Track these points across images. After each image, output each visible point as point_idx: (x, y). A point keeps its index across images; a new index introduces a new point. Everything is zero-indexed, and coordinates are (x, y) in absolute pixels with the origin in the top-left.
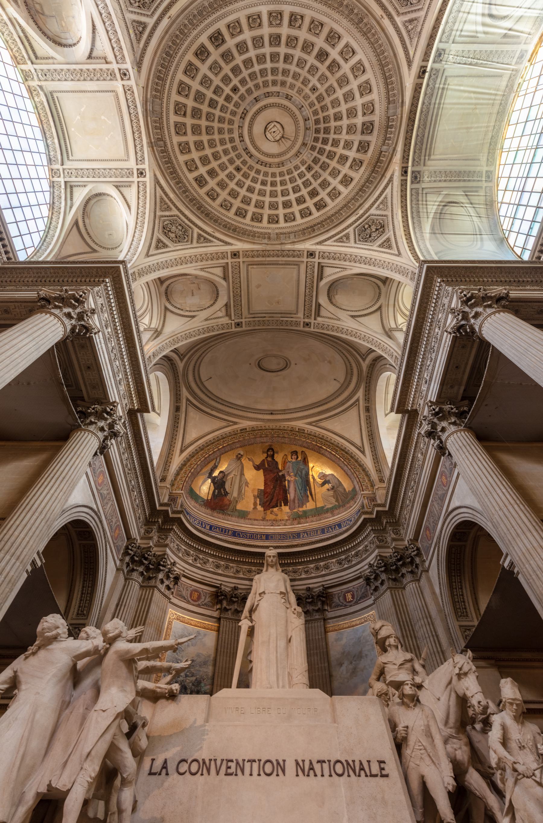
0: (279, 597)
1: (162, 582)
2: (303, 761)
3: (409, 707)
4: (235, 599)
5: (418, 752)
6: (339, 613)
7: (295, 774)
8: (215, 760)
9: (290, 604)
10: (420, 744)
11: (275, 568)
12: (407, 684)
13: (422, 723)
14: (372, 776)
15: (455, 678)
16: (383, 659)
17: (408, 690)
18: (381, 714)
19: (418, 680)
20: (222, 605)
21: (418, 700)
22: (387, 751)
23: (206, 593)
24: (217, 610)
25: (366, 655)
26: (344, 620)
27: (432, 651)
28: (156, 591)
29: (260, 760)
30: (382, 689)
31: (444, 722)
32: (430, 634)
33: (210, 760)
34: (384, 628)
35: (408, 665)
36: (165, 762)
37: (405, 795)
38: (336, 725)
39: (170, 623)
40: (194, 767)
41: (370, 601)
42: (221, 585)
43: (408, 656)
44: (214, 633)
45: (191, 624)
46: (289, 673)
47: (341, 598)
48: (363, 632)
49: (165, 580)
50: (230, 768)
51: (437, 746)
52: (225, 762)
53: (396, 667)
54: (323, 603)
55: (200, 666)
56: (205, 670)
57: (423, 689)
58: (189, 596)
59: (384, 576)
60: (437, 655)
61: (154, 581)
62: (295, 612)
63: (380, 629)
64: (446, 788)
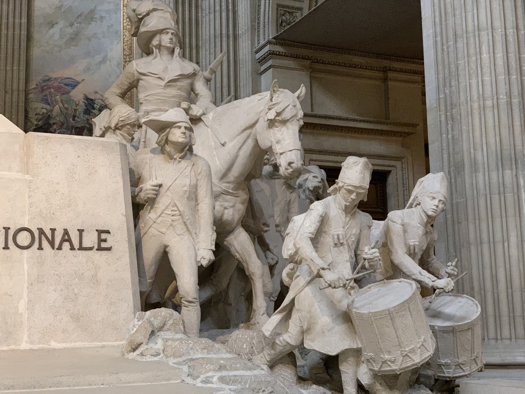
3: (171, 158)
5: (169, 219)
12: (180, 127)
13: (187, 181)
14: (81, 248)
15: (262, 125)
16: (140, 65)
17: (177, 135)
18: (119, 166)
19: (196, 110)
21: (191, 150)
27: (218, 32)
31: (220, 175)
32: (224, 8)
34: (155, 13)
35: (185, 83)
37: (131, 272)
38: (28, 177)
43: (189, 67)
51: (200, 211)
53: (163, 83)
57: (201, 124)
63: (148, 14)
64: (197, 262)
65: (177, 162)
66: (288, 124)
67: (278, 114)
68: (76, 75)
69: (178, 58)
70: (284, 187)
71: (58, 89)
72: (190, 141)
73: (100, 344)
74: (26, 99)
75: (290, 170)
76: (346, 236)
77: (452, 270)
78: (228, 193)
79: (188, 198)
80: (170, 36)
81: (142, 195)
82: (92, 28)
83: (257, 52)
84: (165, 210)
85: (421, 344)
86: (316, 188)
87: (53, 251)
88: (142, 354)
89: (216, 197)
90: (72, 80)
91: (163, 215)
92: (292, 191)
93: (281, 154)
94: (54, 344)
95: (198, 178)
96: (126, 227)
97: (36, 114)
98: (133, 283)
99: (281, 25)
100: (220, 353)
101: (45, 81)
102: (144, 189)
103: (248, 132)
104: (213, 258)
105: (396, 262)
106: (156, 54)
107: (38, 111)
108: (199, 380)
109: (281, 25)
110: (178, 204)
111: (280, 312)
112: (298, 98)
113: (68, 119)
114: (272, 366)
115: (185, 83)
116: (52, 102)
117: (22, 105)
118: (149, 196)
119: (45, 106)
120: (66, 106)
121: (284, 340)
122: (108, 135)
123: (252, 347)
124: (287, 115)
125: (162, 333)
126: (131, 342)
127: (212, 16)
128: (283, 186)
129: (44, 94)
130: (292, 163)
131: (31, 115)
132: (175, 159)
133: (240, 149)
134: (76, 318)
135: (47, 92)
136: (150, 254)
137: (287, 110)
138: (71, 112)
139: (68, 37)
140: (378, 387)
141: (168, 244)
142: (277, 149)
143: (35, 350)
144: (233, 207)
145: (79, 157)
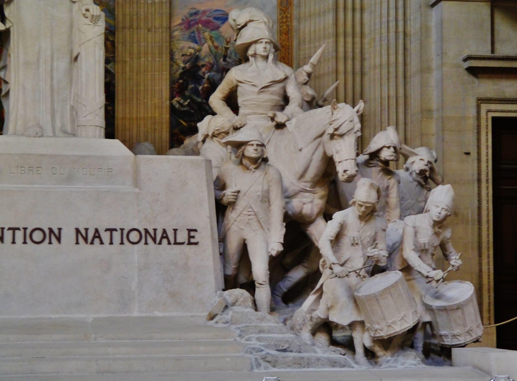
2: (87, 230)
3: (248, 169)
7: (75, 241)
10: (251, 210)
12: (252, 145)
13: (260, 188)
14: (176, 243)
17: (250, 152)
18: (204, 179)
19: (281, 117)
21: (265, 160)
22: (204, 217)
29: (25, 229)
30: (223, 128)
31: (298, 176)
34: (251, 23)
35: (277, 88)
37: (214, 261)
38: (137, 190)
43: (281, 71)
46: (72, 108)
53: (256, 90)
65: (252, 172)
66: (346, 138)
67: (336, 130)
68: (226, 6)
69: (272, 64)
70: (381, 173)
71: (207, 24)
72: (263, 155)
73: (190, 314)
74: (171, 37)
76: (360, 237)
77: (455, 262)
79: (261, 201)
84: (243, 211)
85: (401, 318)
86: (422, 173)
87: (155, 246)
88: (217, 322)
89: (288, 197)
90: (221, 13)
91: (241, 215)
92: (389, 177)
93: (340, 162)
94: (158, 314)
95: (270, 184)
96: (209, 227)
97: (183, 55)
98: (215, 270)
101: (191, 15)
102: (226, 195)
103: (319, 140)
105: (405, 256)
106: (252, 62)
108: (244, 339)
110: (253, 206)
113: (218, 59)
114: (314, 333)
115: (277, 88)
116: (200, 40)
117: (166, 45)
118: (230, 200)
119: (193, 45)
120: (216, 44)
121: (317, 315)
122: (208, 140)
123: (304, 320)
125: (234, 308)
126: (210, 314)
128: (379, 174)
129: (191, 30)
130: (347, 171)
131: (177, 56)
132: (251, 170)
133: (313, 154)
134: (173, 295)
135: (194, 29)
136: (233, 245)
137: (344, 125)
138: (221, 51)
140: (378, 350)
141: (246, 238)
142: (336, 159)
143: (143, 317)
144: (311, 202)
145: (174, 173)
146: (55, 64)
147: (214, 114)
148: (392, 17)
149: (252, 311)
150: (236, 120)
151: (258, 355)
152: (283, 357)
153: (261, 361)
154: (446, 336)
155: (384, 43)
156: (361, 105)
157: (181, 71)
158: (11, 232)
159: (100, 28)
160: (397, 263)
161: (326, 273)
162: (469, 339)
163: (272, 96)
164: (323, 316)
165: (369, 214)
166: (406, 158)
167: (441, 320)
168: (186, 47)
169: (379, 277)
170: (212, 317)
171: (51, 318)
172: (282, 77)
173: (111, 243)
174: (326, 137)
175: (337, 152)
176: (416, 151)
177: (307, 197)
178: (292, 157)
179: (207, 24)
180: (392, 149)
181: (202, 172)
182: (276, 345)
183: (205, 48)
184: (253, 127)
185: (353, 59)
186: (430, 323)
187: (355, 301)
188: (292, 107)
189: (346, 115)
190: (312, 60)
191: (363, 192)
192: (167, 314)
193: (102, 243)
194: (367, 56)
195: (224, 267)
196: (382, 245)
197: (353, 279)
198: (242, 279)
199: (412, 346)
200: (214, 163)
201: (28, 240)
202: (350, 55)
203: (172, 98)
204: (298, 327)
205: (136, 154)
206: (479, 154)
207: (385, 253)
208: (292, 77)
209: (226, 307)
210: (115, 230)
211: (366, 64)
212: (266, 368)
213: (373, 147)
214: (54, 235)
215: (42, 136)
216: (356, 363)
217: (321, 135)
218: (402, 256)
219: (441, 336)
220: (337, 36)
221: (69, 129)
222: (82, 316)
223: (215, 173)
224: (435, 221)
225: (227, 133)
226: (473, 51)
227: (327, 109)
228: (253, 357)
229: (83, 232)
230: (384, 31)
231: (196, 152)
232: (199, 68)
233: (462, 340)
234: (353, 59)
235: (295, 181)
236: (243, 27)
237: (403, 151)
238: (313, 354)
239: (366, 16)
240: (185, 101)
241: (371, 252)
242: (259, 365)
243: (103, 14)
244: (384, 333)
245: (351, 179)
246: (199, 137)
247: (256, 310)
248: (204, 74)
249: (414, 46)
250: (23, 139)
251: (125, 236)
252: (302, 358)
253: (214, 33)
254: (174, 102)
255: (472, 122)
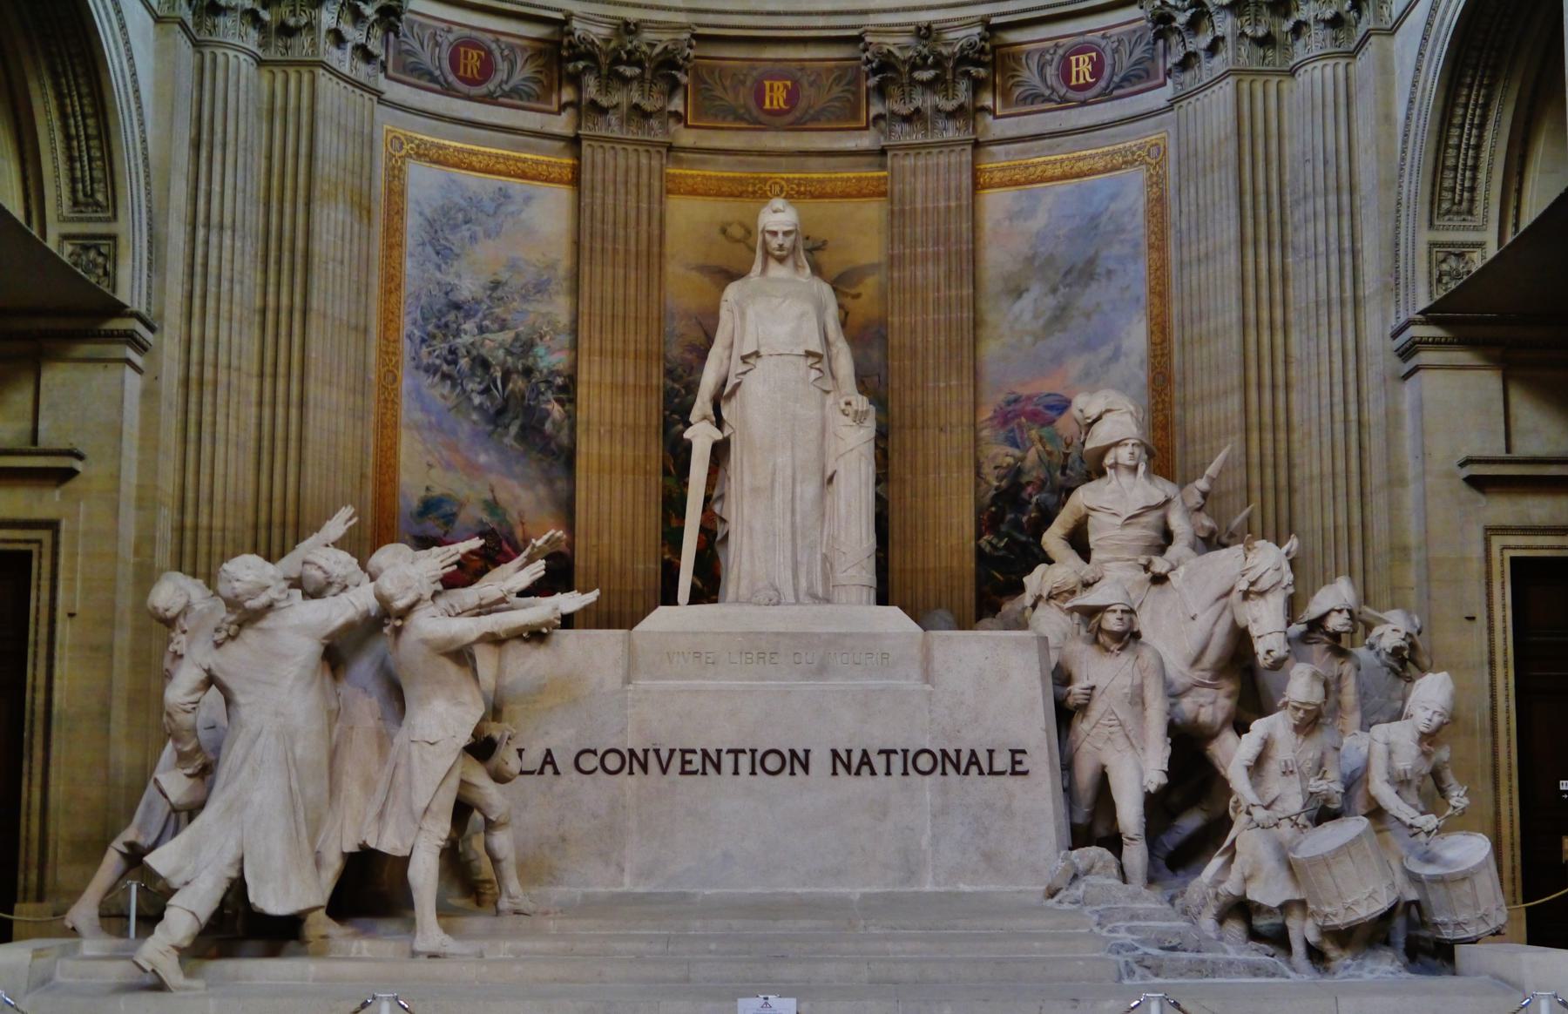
0: (804, 363)
1: (338, 38)
2: (849, 752)
3: (1107, 650)
4: (629, 71)
6: (1032, 124)
8: (657, 752)
9: (834, 377)
11: (790, 262)
13: (1128, 681)
14: (991, 773)
17: (1112, 622)
18: (1037, 667)
19: (1160, 565)
20: (579, 89)
21: (1136, 636)
23: (512, 48)
24: (563, 107)
25: (1110, 273)
26: (1051, 150)
27: (1323, 296)
28: (324, 80)
29: (753, 751)
31: (1191, 659)
32: (1334, 247)
33: (646, 751)
36: (549, 752)
38: (928, 687)
39: (395, 174)
40: (613, 762)
41: (1157, 98)
42: (569, 16)
43: (1159, 490)
44: (564, 193)
45: (471, 168)
46: (825, 558)
47: (1051, 72)
48: (1113, 197)
49: (348, 30)
50: (690, 762)
52: (677, 755)
53: (1119, 521)
54: (977, 86)
55: (524, 298)
56: (544, 309)
58: (446, 64)
59: (1225, 25)
60: (1336, 309)
61: (305, 40)
62: (849, 410)
63: (1099, 418)
66: (1269, 597)
67: (1253, 584)
71: (1034, 416)
73: (1015, 888)
74: (977, 440)
75: (1270, 661)
78: (1204, 685)
80: (1128, 449)
81: (1071, 700)
82: (1094, 295)
83: (1395, 336)
86: (1396, 652)
87: (959, 777)
88: (1060, 902)
89: (1174, 695)
94: (964, 887)
99: (1439, 281)
100: (1151, 901)
101: (1008, 403)
103: (1223, 601)
104: (1164, 780)
105: (1373, 793)
107: (999, 461)
109: (1439, 281)
111: (1222, 854)
112: (1287, 554)
114: (1221, 920)
116: (1023, 443)
119: (1011, 450)
122: (1040, 604)
124: (1263, 584)
125: (1088, 878)
126: (1048, 888)
127: (1311, 263)
131: (987, 469)
133: (1215, 624)
134: (988, 857)
135: (1014, 425)
136: (1085, 775)
139: (1048, 314)
142: (1254, 631)
144: (1213, 703)
146: (798, 489)
147: (1050, 562)
148: (1338, 398)
149: (1119, 883)
150: (1087, 571)
151: (1129, 957)
152: (1172, 960)
153: (1135, 967)
154: (1445, 925)
155: (1327, 440)
156: (1293, 544)
157: (993, 492)
158: (732, 756)
159: (868, 431)
160: (1360, 804)
161: (1240, 820)
162: (1483, 929)
163: (1145, 531)
164: (1235, 892)
165: (1310, 723)
166: (1369, 627)
167: (1435, 897)
168: (1000, 454)
169: (1329, 828)
170: (1052, 894)
171: (794, 894)
172: (1161, 499)
173: (888, 773)
174: (1236, 597)
175: (1255, 621)
176: (1385, 616)
177: (1206, 695)
178: (1180, 628)
179: (1034, 416)
180: (1345, 614)
181: (1033, 657)
182: (1159, 941)
183: (1032, 456)
184: (1115, 583)
185: (1275, 466)
186: (1417, 903)
187: (1291, 867)
188: (1178, 549)
189: (1267, 559)
190: (1208, 472)
191: (1300, 686)
192: (979, 889)
193: (873, 773)
194: (1297, 461)
195: (1071, 811)
196: (1333, 774)
197: (1286, 830)
198: (1101, 830)
199: (1387, 942)
200: (1052, 641)
201: (758, 769)
202: (1269, 459)
203: (979, 536)
204: (1194, 910)
205: (925, 630)
206: (1490, 618)
207: (1338, 787)
208: (1178, 499)
209: (1075, 877)
210: (895, 752)
211: (1297, 473)
212: (1143, 977)
213: (1314, 610)
214: (798, 761)
215: (778, 603)
216: (1294, 970)
217: (1228, 594)
218: (1368, 791)
219: (1436, 924)
220: (1247, 430)
221: (820, 591)
222: (842, 890)
223: (1054, 658)
224: (1422, 733)
225: (1073, 592)
226: (1476, 448)
227: (1237, 549)
228: (1121, 959)
229: (844, 756)
230: (1326, 420)
231: (1021, 624)
232: (1022, 487)
233: (1471, 932)
234: (1275, 466)
235: (1185, 669)
236: (1095, 421)
237: (1363, 617)
238: (1221, 955)
239: (1295, 397)
240: (1001, 540)
241: (1315, 785)
242: (1131, 973)
243: (872, 409)
244: (1340, 920)
245: (1278, 665)
246: (1028, 598)
247: (1125, 881)
248: (1031, 496)
249: (1375, 444)
250: (748, 608)
251: (910, 761)
252: (1203, 961)
253: (1045, 431)
254: (983, 542)
255: (1477, 566)
